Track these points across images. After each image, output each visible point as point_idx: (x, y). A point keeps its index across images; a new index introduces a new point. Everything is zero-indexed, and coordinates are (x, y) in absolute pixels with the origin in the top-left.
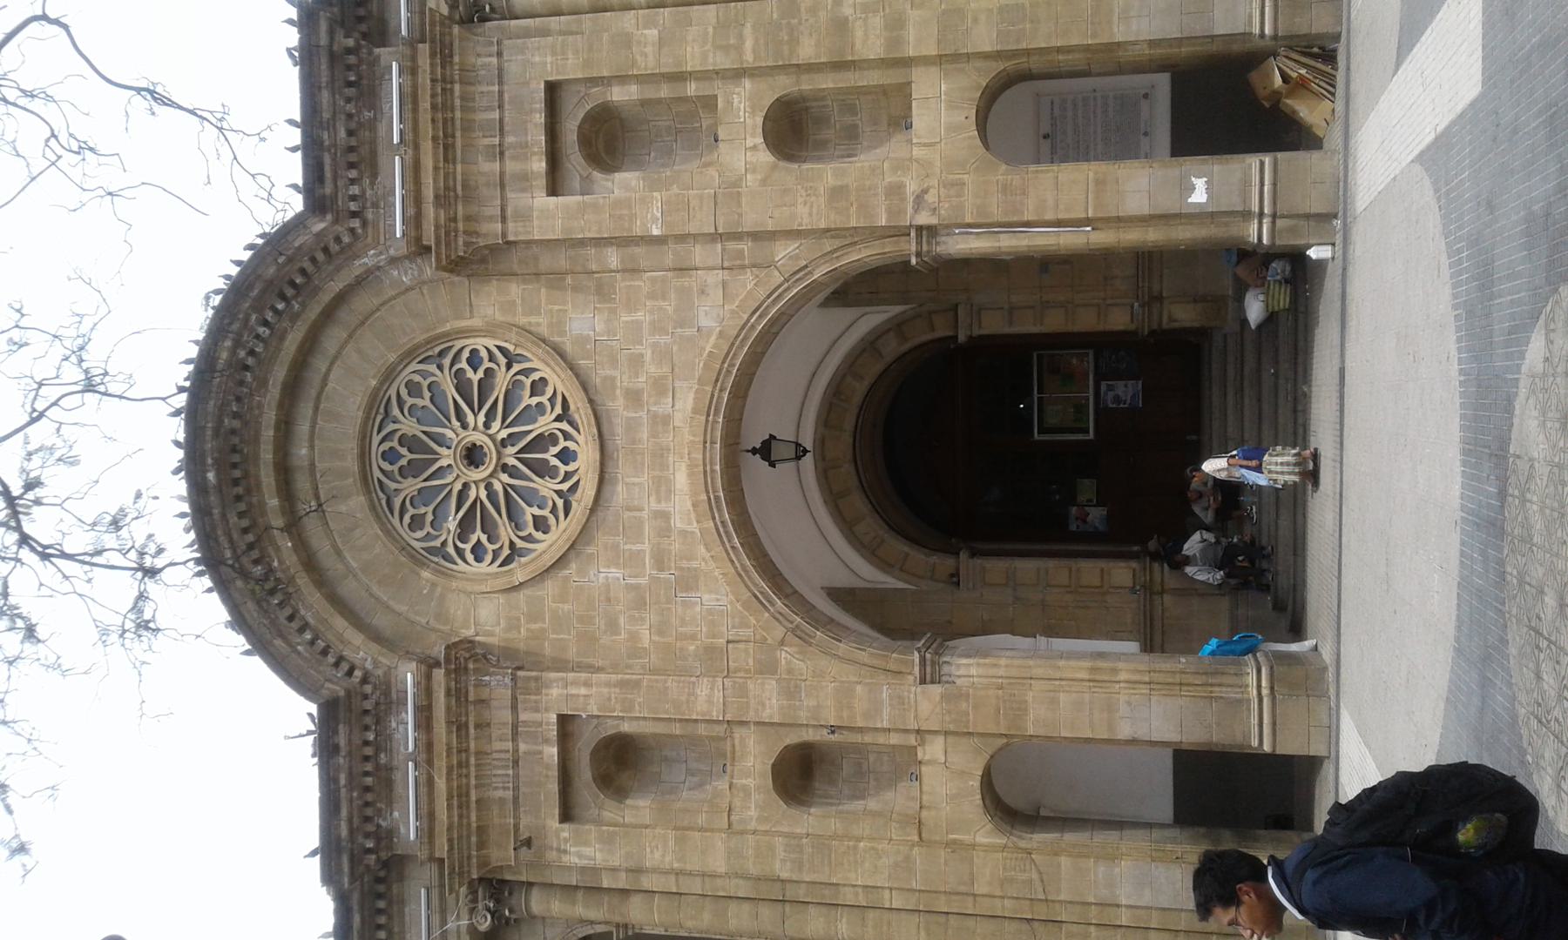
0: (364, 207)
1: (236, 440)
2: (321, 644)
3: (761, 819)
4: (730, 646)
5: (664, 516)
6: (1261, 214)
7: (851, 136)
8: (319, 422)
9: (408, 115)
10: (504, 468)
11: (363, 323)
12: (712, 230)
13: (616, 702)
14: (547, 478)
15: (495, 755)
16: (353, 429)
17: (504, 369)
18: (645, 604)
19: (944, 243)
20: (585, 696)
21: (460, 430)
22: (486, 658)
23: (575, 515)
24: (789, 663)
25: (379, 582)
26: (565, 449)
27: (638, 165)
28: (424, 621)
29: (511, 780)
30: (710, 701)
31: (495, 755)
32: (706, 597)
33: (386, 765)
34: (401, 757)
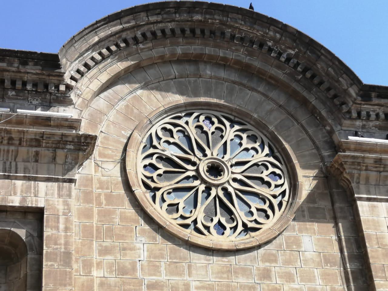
0: (362, 120)
1: (218, 34)
8: (226, 83)
11: (289, 114)
13: (54, 249)
14: (204, 215)
15: (13, 164)
18: (123, 275)
20: (57, 228)
21: (230, 164)
23: (183, 230)
25: (127, 106)
26: (224, 228)
31: (13, 164)
33: (7, 94)
34: (11, 105)
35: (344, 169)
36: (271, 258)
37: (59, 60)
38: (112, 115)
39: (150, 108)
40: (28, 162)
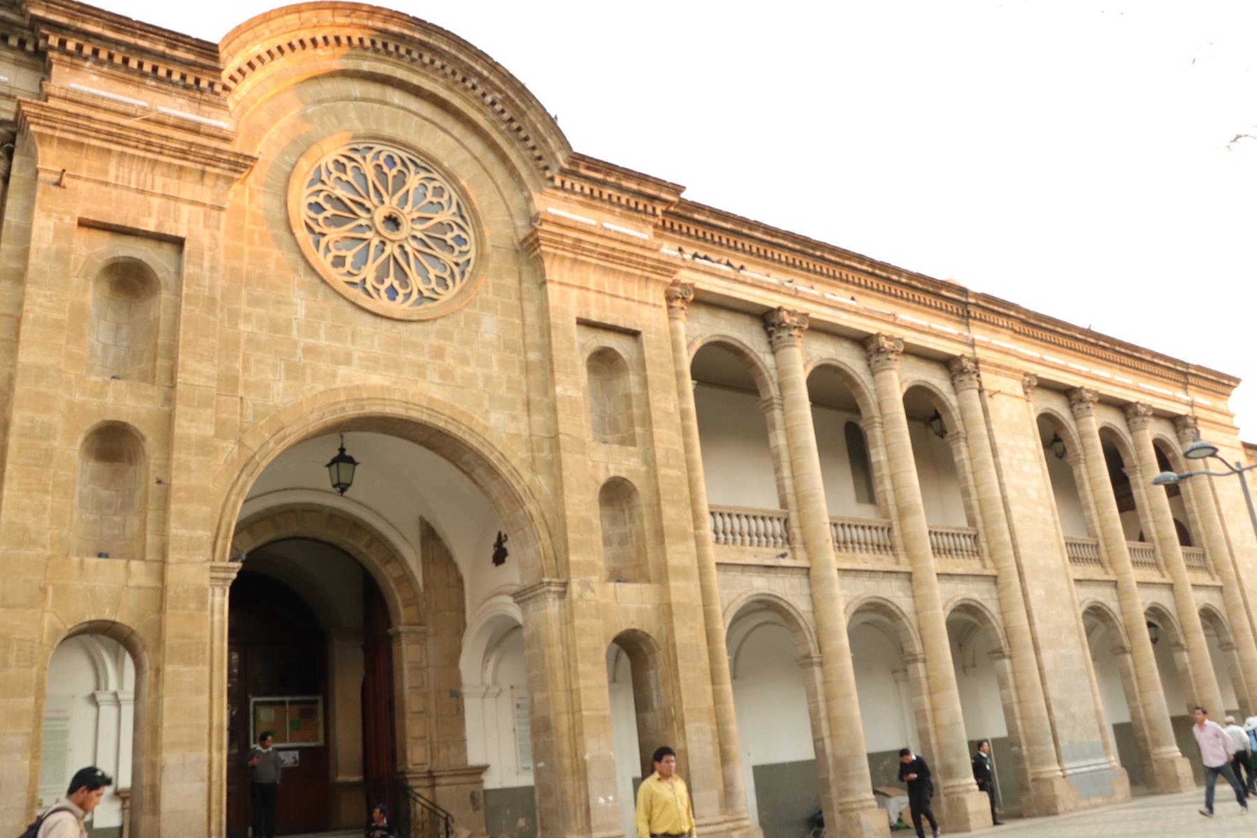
1: (415, 55)
4: (238, 399)
5: (348, 361)
8: (416, 119)
9: (620, 237)
10: (383, 243)
11: (484, 169)
12: (561, 430)
15: (149, 177)
16: (412, 139)
20: (201, 266)
24: (224, 449)
26: (397, 293)
29: (126, 184)
31: (149, 177)
34: (149, 98)
35: (539, 245)
36: (446, 335)
37: (218, 52)
38: (272, 133)
40: (168, 177)
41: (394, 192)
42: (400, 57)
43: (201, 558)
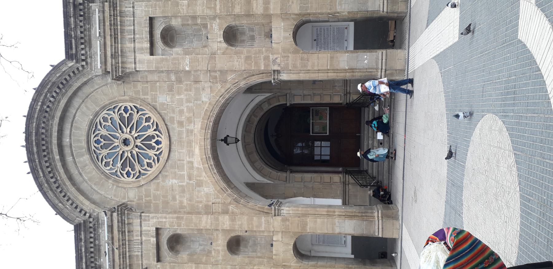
0: (86, 58)
2: (74, 205)
3: (222, 260)
4: (213, 205)
5: (192, 163)
6: (382, 69)
7: (252, 38)
8: (73, 130)
10: (137, 146)
14: (151, 150)
15: (135, 241)
16: (84, 133)
17: (136, 113)
18: (185, 191)
19: (282, 76)
20: (165, 222)
21: (121, 134)
22: (132, 210)
24: (232, 210)
25: (95, 184)
26: (157, 140)
27: (181, 45)
28: (110, 197)
29: (140, 249)
30: (206, 223)
31: (135, 241)
32: (205, 189)
33: (98, 244)
34: (103, 242)
35: (119, 75)
37: (77, 224)
39: (94, 173)
40: (133, 235)
41: (113, 141)
42: (47, 142)
43: (272, 220)
